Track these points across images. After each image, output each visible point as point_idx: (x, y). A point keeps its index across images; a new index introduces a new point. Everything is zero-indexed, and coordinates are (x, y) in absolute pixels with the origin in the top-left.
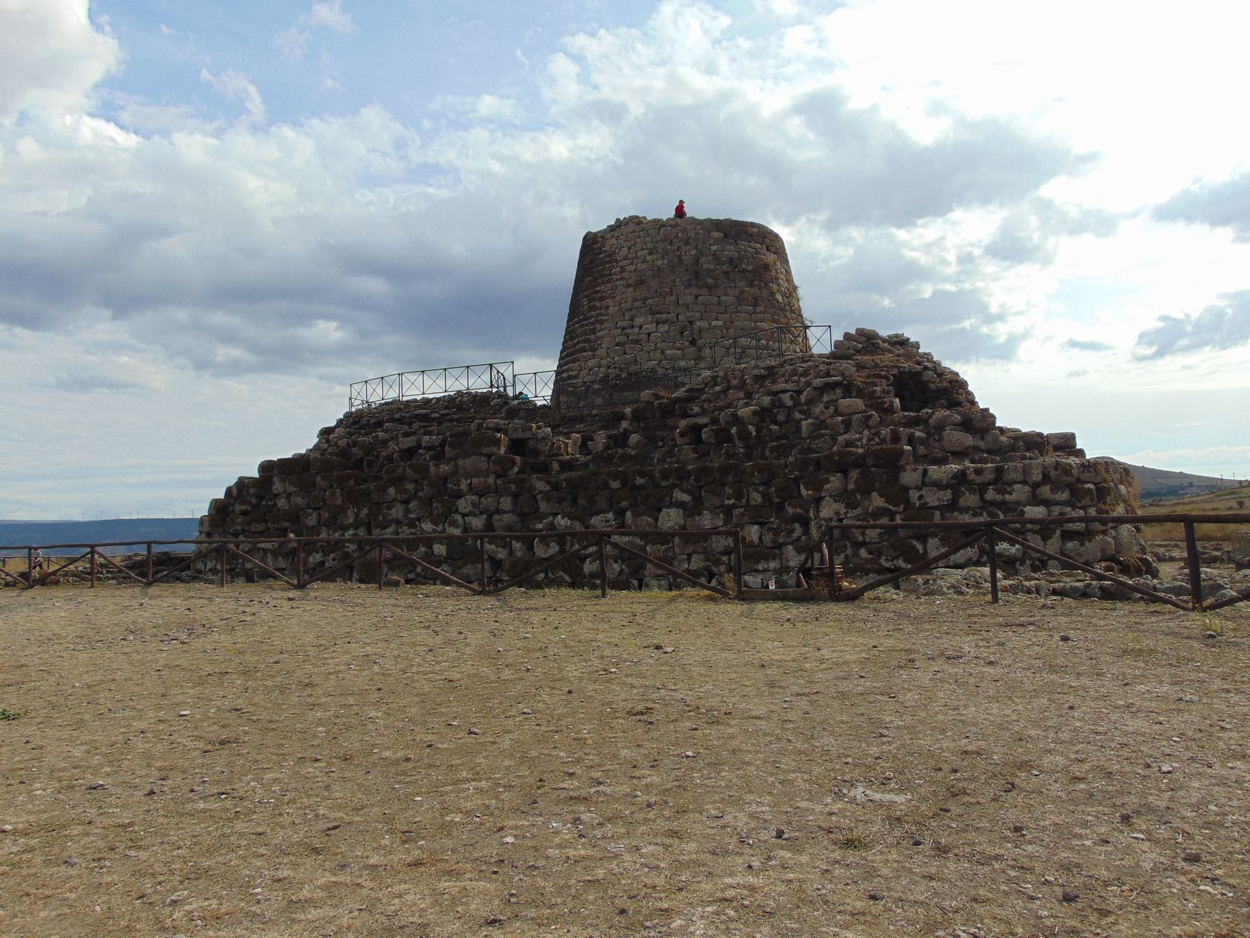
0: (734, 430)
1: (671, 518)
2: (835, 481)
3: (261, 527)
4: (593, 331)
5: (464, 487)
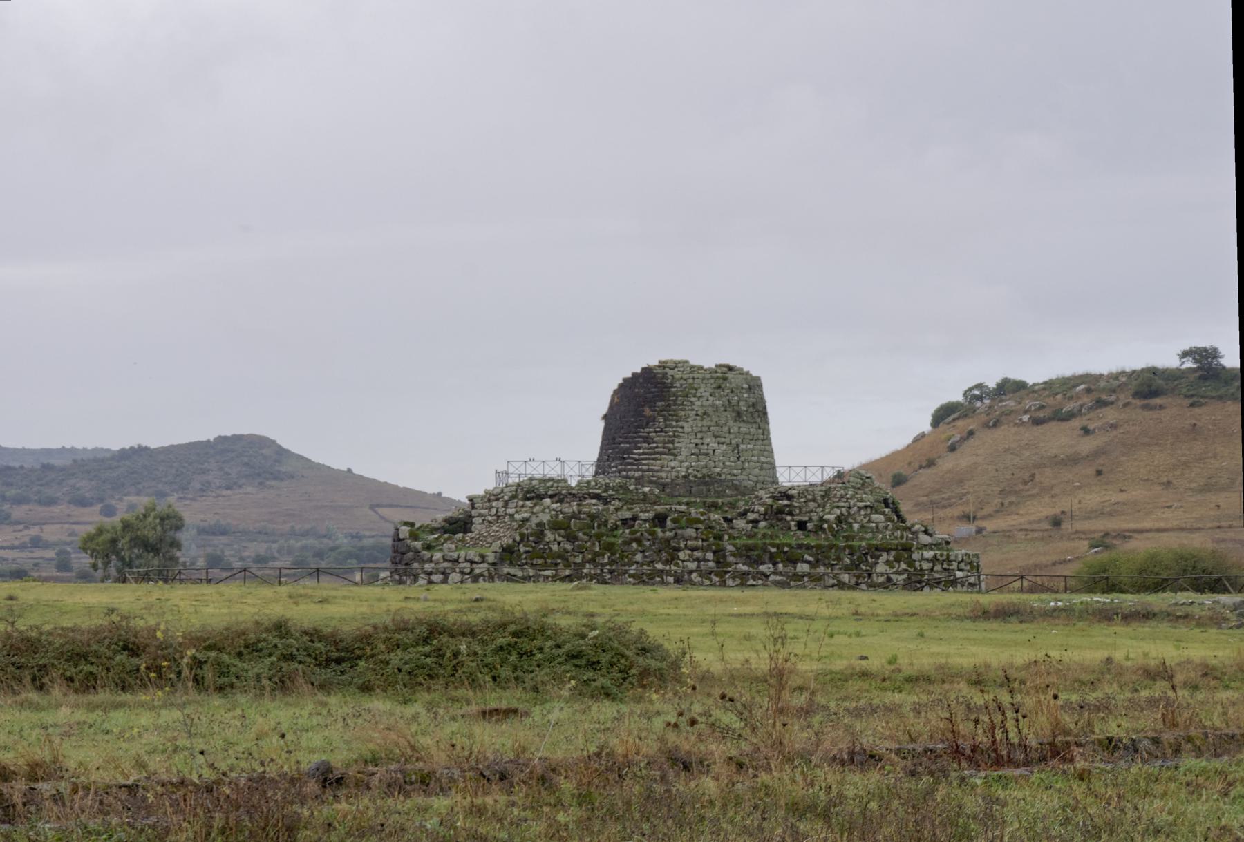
0: (825, 526)
1: (803, 568)
2: (885, 554)
3: (540, 561)
4: (672, 442)
5: (682, 545)
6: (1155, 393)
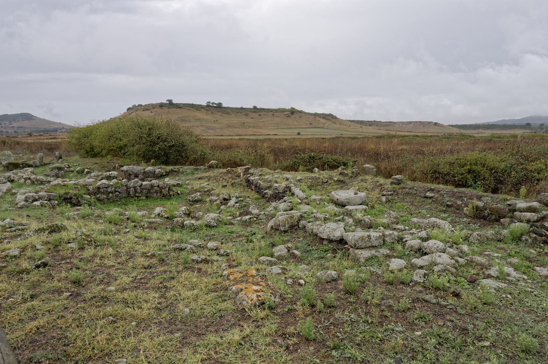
6: (162, 106)
